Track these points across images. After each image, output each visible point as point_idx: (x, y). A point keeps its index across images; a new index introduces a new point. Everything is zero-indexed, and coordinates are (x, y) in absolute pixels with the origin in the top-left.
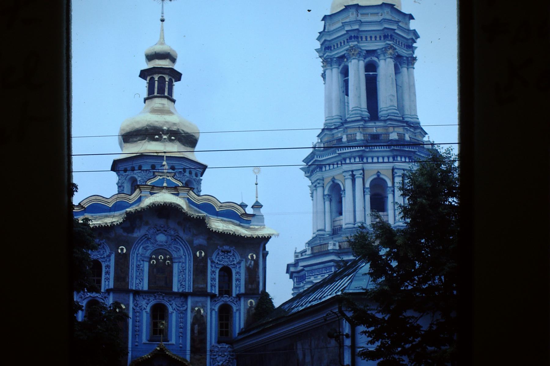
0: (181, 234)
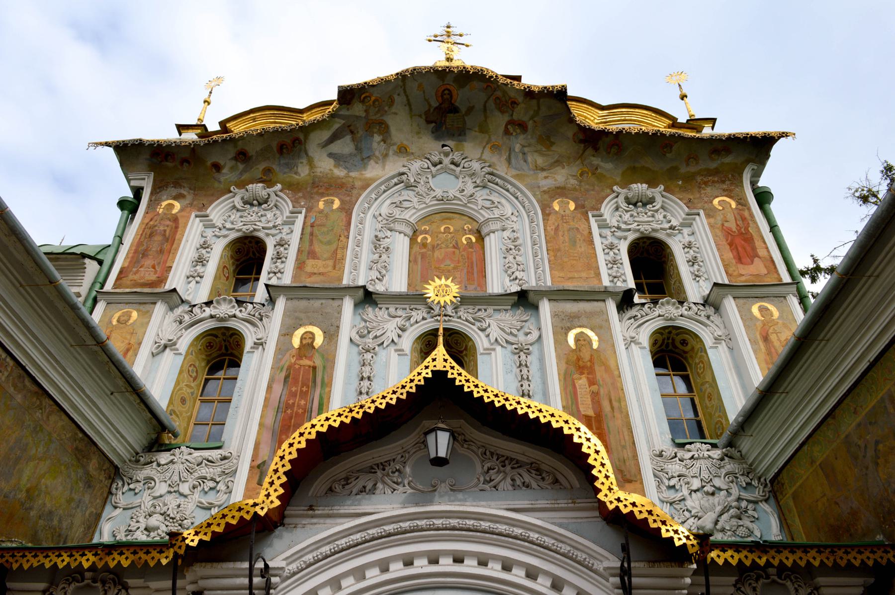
0: (502, 169)
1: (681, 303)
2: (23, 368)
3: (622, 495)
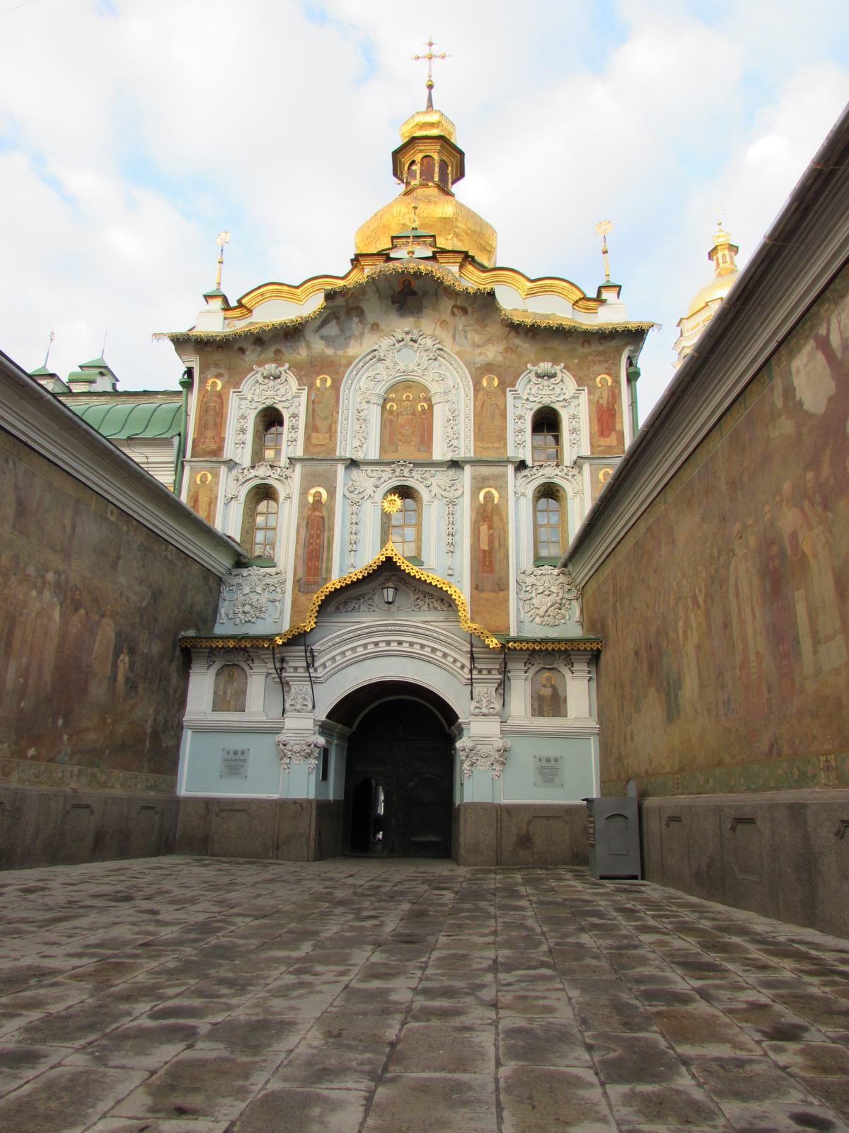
0: (448, 346)
1: (557, 466)
2: (178, 549)
3: (471, 625)
